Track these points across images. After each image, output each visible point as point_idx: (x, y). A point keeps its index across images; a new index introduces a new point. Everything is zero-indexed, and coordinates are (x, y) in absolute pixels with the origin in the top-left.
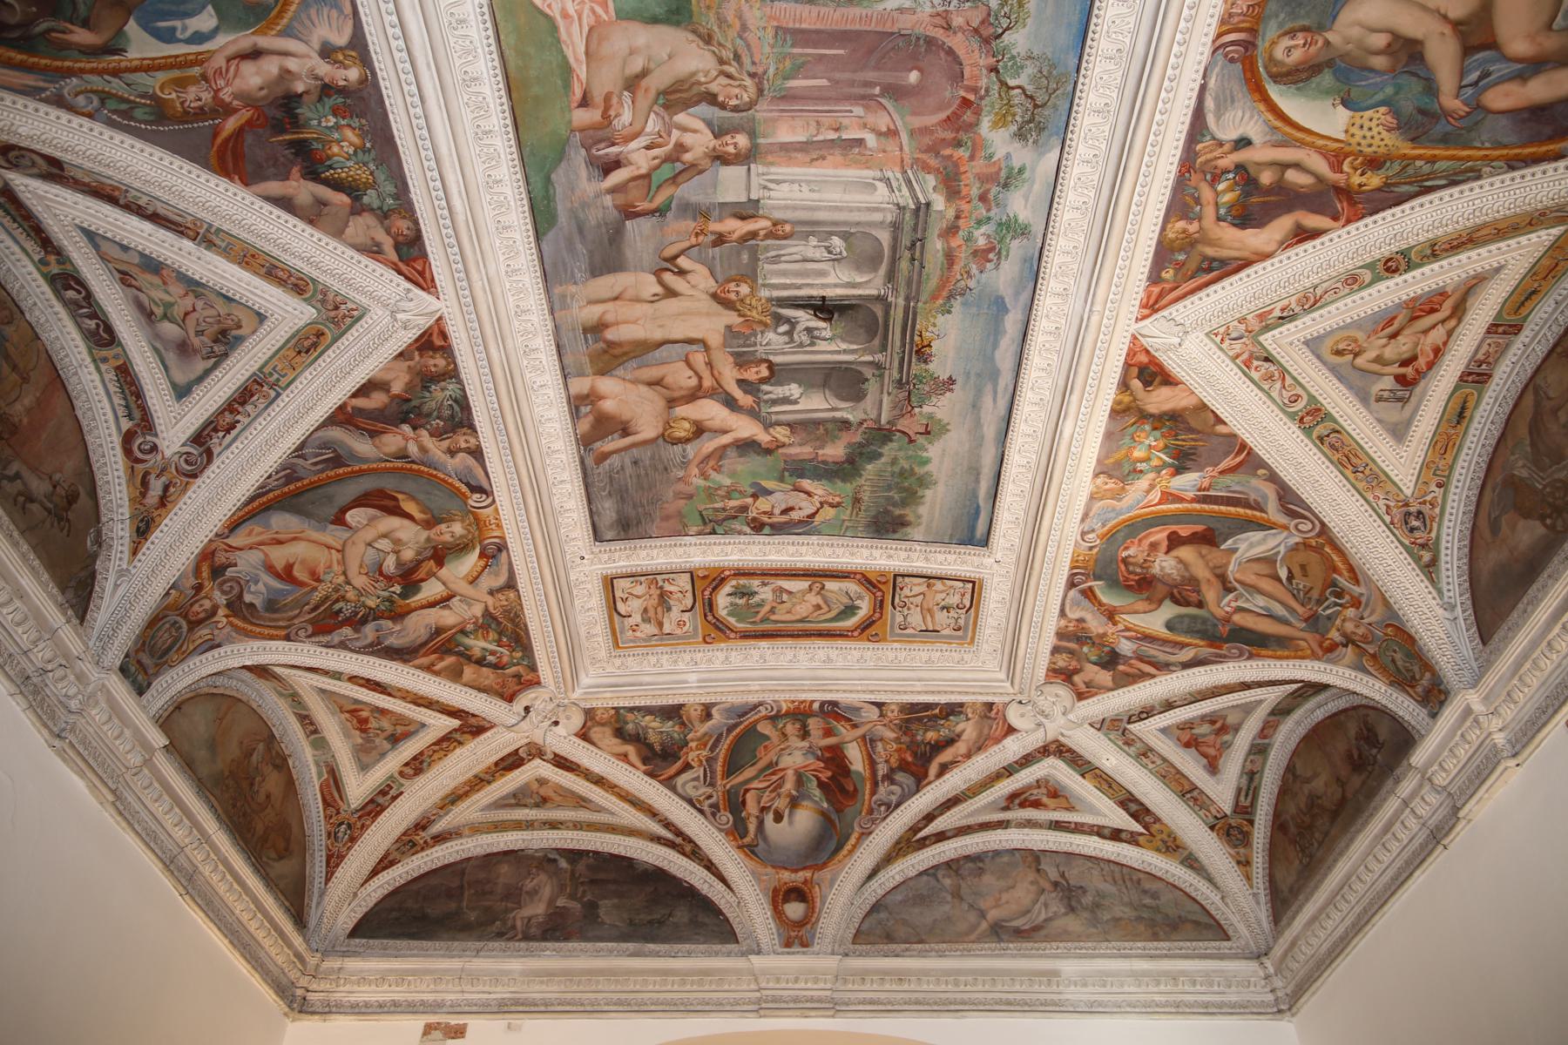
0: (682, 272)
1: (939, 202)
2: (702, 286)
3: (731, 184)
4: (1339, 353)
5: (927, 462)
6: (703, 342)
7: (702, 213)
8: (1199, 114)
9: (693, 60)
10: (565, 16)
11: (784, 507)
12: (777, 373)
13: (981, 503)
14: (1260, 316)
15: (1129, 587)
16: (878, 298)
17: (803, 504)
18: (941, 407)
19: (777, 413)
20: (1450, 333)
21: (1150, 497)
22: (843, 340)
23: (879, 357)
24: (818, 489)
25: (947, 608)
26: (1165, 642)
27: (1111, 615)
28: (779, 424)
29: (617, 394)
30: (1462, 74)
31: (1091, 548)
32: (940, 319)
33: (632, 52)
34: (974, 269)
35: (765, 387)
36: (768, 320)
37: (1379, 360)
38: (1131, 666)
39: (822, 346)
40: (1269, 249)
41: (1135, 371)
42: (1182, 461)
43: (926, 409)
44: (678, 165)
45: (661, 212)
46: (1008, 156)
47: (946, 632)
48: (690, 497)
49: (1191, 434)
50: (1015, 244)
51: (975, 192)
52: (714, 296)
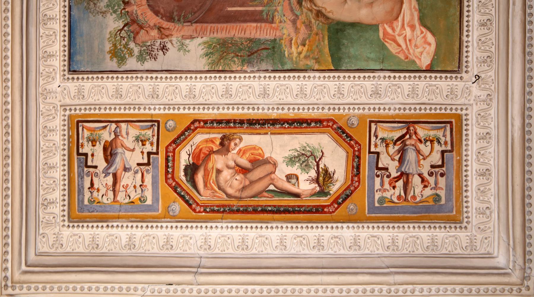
10: (413, 27)
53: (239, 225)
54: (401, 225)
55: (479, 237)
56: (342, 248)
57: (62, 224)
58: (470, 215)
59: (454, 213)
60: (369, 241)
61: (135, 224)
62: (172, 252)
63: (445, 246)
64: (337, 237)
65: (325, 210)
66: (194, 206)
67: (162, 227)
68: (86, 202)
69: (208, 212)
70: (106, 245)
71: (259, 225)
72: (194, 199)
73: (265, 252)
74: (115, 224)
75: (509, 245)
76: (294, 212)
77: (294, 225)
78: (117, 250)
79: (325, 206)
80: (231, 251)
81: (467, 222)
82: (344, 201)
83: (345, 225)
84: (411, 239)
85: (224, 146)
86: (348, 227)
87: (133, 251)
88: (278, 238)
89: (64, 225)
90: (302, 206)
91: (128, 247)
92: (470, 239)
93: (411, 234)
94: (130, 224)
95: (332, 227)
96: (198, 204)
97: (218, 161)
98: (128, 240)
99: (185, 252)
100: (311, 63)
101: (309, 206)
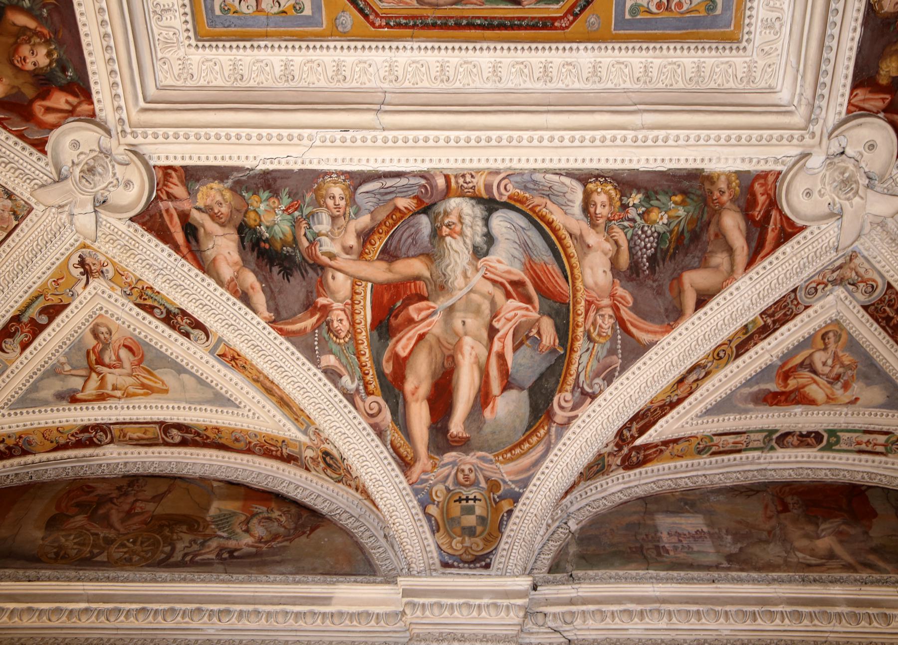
53: (436, 45)
54: (658, 46)
55: (761, 63)
56: (576, 80)
57: (187, 43)
58: (753, 29)
59: (732, 28)
60: (613, 70)
61: (290, 44)
62: (346, 85)
63: (715, 77)
64: (570, 64)
65: (557, 24)
66: (371, 17)
67: (328, 47)
68: (218, 12)
69: (392, 27)
70: (253, 76)
71: (464, 45)
72: (371, 7)
73: (472, 85)
74: (262, 44)
75: (798, 71)
76: (512, 27)
77: (512, 46)
78: (269, 84)
79: (555, 19)
80: (426, 84)
81: (747, 41)
82: (583, 10)
83: (582, 46)
84: (669, 67)
86: (586, 48)
87: (293, 84)
88: (490, 65)
89: (190, 45)
90: (524, 18)
91: (284, 79)
92: (749, 66)
93: (670, 60)
94: (283, 44)
95: (564, 49)
96: (377, 15)
98: (283, 68)
99: (363, 86)
101: (533, 18)
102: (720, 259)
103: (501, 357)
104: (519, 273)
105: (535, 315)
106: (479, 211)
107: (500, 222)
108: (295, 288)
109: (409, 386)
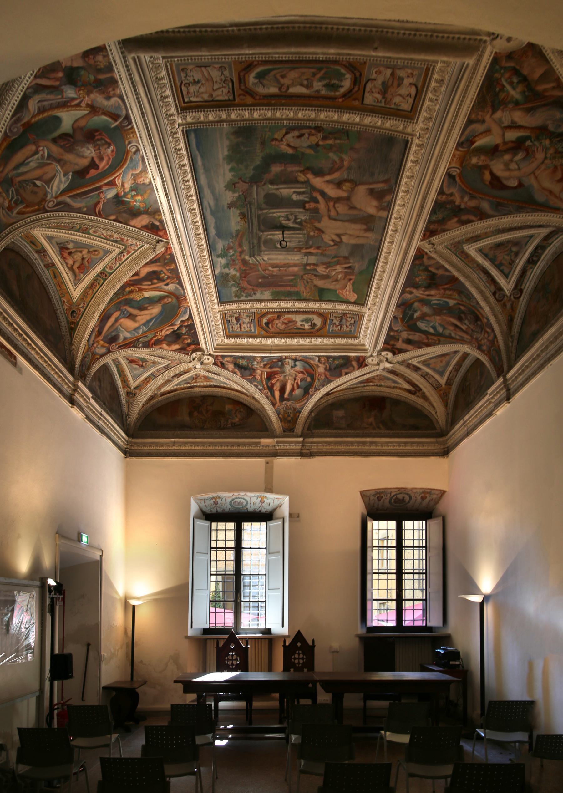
0: (333, 241)
1: (247, 258)
2: (327, 236)
3: (312, 260)
4: (95, 251)
5: (231, 170)
6: (330, 218)
7: (322, 254)
8: (182, 286)
9: (320, 283)
10: (350, 292)
11: (303, 138)
12: (302, 204)
13: (197, 153)
14: (130, 252)
15: (96, 130)
16: (263, 232)
17: (292, 140)
18: (229, 197)
19: (303, 188)
20: (67, 264)
21: (120, 181)
22: (275, 217)
23: (260, 212)
24: (284, 148)
25: (196, 82)
26: (52, 108)
27: (94, 109)
28: (302, 183)
29: (370, 207)
30: (128, 312)
31: (130, 143)
32: (239, 228)
33: (335, 285)
34: (231, 244)
35: (307, 199)
36: (304, 223)
37: (81, 252)
38: (57, 79)
39: (283, 214)
40: (142, 269)
41: (160, 228)
42: (118, 200)
43: (236, 195)
44: (328, 265)
45: (335, 257)
46: (229, 270)
47: (191, 67)
48: (352, 148)
49: (123, 210)
50: (220, 252)
51: (237, 262)
52: (323, 232)
85: (279, 318)
97: (277, 322)
100: (311, 298)
102: (352, 368)
103: (297, 383)
104: (302, 370)
105: (305, 376)
106: (293, 361)
107: (297, 363)
108: (247, 372)
109: (275, 388)
